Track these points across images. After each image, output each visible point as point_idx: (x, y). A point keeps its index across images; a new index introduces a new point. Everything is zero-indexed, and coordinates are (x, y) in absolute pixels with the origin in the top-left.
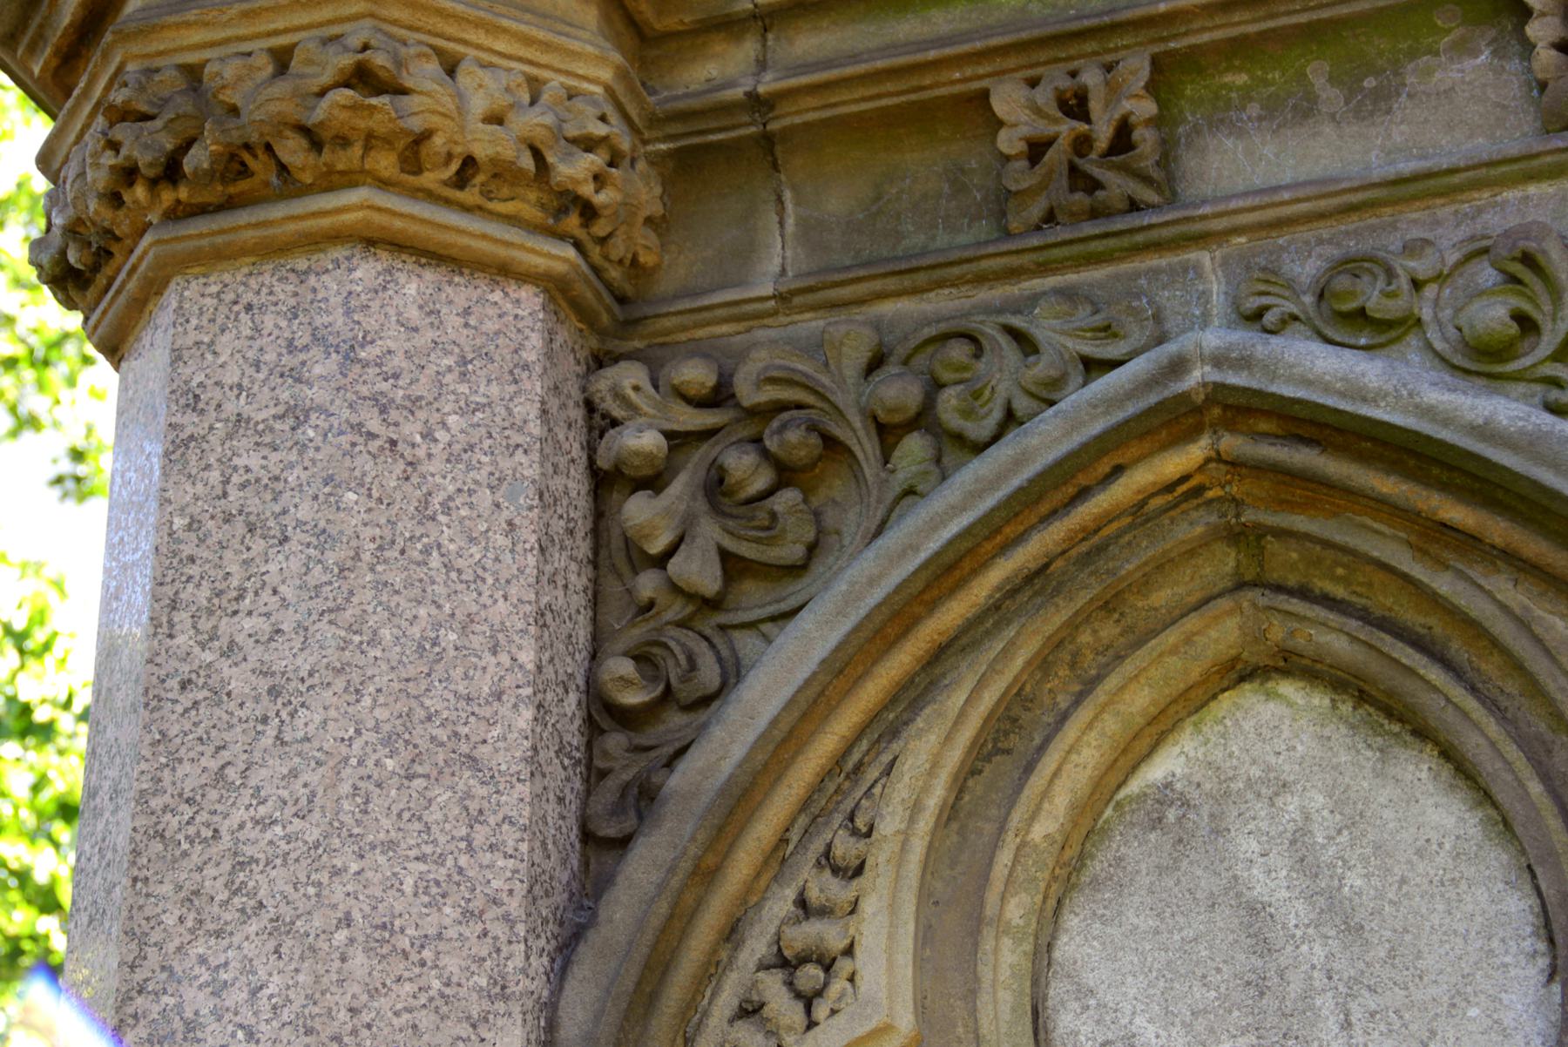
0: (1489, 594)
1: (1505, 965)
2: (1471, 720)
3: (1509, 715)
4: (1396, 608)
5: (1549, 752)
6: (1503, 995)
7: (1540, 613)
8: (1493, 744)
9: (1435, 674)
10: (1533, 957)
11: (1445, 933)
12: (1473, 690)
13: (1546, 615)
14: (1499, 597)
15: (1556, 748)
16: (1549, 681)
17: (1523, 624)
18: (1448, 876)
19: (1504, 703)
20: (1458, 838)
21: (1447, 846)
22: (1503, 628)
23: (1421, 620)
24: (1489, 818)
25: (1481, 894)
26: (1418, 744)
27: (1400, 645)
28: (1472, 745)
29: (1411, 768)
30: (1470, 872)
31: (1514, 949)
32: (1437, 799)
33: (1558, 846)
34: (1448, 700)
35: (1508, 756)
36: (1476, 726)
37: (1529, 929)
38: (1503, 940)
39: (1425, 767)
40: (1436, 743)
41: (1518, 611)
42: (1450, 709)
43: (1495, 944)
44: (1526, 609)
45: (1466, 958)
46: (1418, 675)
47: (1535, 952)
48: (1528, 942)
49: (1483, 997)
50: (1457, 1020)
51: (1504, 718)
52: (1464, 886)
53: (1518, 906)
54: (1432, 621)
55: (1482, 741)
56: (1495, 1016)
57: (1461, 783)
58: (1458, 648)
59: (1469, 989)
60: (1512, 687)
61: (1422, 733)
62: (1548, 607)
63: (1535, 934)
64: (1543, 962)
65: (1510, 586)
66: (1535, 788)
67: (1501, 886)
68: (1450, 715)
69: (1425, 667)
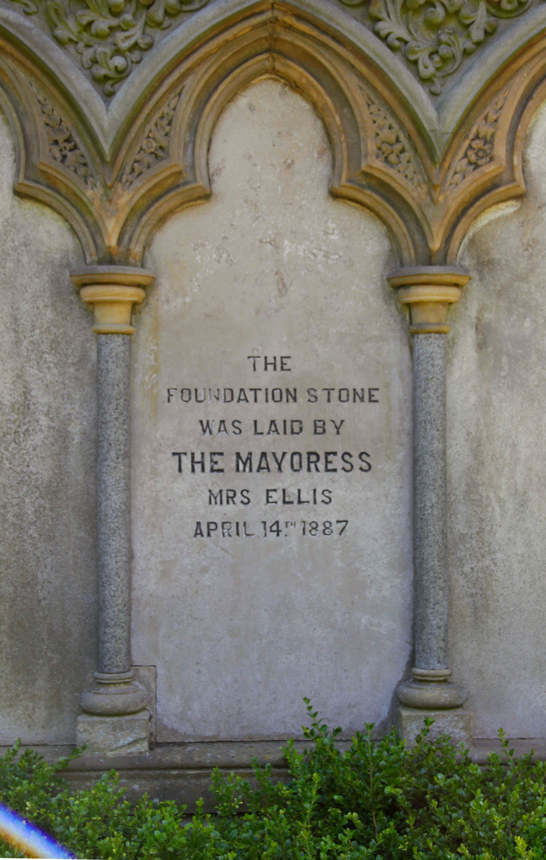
17: (14, 73)
22: (9, 72)
53: (9, 142)
64: (13, 157)
66: (14, 115)
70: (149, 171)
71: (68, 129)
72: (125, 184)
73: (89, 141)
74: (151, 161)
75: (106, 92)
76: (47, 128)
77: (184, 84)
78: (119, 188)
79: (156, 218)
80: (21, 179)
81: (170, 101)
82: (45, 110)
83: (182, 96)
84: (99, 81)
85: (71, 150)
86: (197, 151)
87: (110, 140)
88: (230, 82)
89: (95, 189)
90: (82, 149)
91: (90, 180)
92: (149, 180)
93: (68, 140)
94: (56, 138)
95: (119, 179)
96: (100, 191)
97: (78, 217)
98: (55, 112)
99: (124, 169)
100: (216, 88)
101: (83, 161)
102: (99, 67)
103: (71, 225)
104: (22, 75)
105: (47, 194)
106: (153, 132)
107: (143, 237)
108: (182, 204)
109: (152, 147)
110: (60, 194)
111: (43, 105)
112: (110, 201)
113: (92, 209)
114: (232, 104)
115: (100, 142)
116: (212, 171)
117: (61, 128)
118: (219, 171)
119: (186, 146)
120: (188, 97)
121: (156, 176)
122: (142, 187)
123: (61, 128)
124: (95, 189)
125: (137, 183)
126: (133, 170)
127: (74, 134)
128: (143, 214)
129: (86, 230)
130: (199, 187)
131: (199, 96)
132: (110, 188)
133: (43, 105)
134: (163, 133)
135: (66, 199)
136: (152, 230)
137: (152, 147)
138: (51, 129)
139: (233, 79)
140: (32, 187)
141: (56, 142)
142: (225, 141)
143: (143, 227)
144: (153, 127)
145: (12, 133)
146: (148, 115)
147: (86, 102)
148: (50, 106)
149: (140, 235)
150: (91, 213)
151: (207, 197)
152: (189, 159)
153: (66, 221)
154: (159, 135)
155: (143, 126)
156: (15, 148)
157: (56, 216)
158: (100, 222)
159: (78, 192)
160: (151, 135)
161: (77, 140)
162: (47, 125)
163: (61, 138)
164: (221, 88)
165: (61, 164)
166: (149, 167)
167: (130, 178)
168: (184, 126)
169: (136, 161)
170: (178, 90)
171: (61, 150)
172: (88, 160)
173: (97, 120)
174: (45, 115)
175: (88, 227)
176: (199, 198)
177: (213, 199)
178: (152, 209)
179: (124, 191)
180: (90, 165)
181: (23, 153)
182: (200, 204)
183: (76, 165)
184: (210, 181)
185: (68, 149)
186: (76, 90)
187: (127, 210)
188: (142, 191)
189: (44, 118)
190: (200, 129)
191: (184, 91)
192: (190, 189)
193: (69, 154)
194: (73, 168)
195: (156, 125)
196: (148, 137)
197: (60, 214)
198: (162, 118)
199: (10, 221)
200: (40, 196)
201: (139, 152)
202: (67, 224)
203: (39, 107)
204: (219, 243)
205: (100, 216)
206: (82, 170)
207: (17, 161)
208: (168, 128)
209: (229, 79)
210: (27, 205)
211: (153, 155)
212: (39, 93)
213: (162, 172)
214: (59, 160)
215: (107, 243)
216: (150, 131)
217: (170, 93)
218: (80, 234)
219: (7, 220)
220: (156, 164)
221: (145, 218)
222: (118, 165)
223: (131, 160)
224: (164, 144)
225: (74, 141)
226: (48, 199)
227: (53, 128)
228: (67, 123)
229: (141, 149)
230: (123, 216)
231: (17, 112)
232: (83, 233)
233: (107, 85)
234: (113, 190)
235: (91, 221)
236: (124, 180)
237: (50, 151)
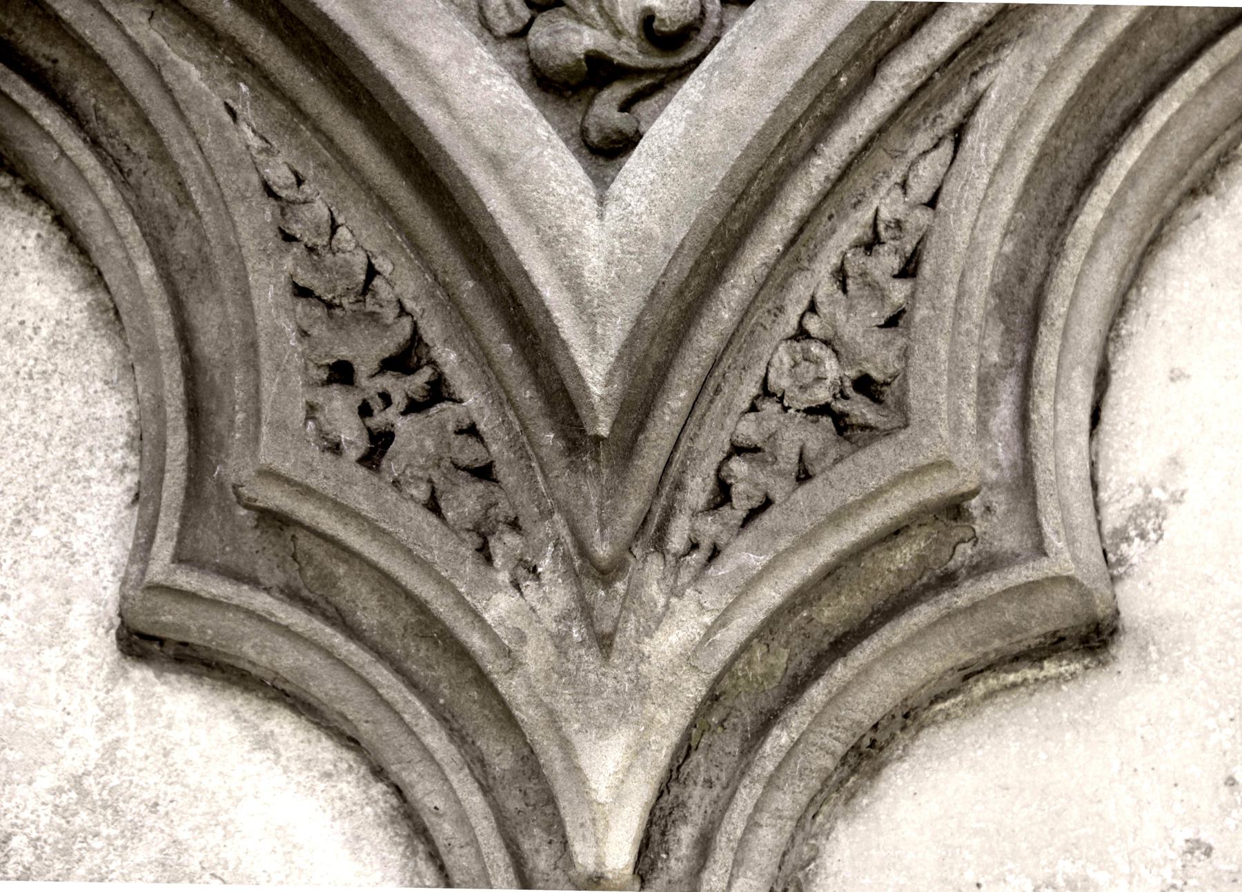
0: (118, 25)
1: (88, 480)
2: (86, 180)
3: (132, 180)
4: (18, 31)
5: (172, 229)
6: (78, 515)
7: (174, 56)
8: (106, 212)
9: (50, 118)
10: (122, 472)
11: (23, 436)
12: (94, 144)
13: (180, 60)
14: (129, 31)
15: (180, 225)
16: (174, 141)
17: (154, 69)
18: (39, 368)
19: (129, 164)
20: (58, 323)
21: (44, 332)
22: (130, 70)
23: (46, 50)
24: (99, 303)
25: (75, 394)
26: (29, 204)
27: (14, 76)
28: (84, 210)
29: (16, 233)
30: (65, 364)
31: (101, 461)
32: (41, 273)
33: (160, 342)
34: (63, 153)
35: (121, 229)
36: (91, 188)
37: (122, 439)
38: (90, 450)
39: (33, 233)
40: (52, 207)
41: (148, 51)
42: (64, 163)
43: (81, 453)
44: (159, 49)
45: (42, 467)
46: (30, 116)
47: (125, 466)
48: (120, 453)
49: (54, 515)
50: (19, 540)
51: (126, 182)
52: (55, 381)
53: (114, 411)
54: (58, 53)
55: (95, 206)
56: (65, 539)
57: (73, 258)
58: (84, 91)
59: (40, 505)
60: (140, 145)
61: (35, 192)
62: (184, 50)
63: (129, 446)
64: (131, 479)
65: (144, 19)
66: (146, 269)
67: (99, 385)
68: (63, 172)
69: (39, 108)
70: (801, 494)
71: (403, 312)
72: (680, 557)
73: (505, 350)
74: (813, 447)
75: (594, 136)
76: (301, 306)
77: (981, 84)
78: (652, 575)
79: (835, 741)
80: (160, 566)
81: (913, 164)
82: (296, 229)
83: (970, 139)
84: (561, 86)
85: (414, 407)
86: (1043, 407)
87: (615, 333)
88: (1203, 89)
89: (529, 586)
90: (472, 400)
91: (505, 545)
92: (808, 539)
93: (404, 360)
94: (344, 353)
95: (652, 532)
96: (553, 595)
97: (436, 740)
98: (343, 232)
99: (679, 486)
100: (1134, 117)
101: (470, 453)
102: (565, 23)
103: (398, 791)
104: (192, 72)
105: (286, 631)
106: (824, 309)
107: (769, 838)
108: (969, 674)
109: (819, 379)
110: (353, 632)
111: (284, 205)
112: (604, 643)
113: (511, 687)
114: (1207, 205)
115: (564, 345)
116: (1113, 517)
117: (370, 306)
118: (1148, 519)
119: (987, 386)
120: (999, 144)
121: (837, 518)
122: (765, 574)
123: (370, 306)
124: (529, 586)
125: (745, 556)
126: (723, 493)
127: (432, 331)
128: (767, 721)
129: (475, 802)
130: (1055, 580)
131: (1045, 156)
132: (606, 575)
133: (284, 205)
134: (877, 315)
135: (382, 654)
136: (814, 805)
137: (819, 379)
138: (319, 312)
139: (1217, 76)
140: (214, 602)
141: (342, 373)
142: (1176, 376)
143: (771, 783)
144: (826, 289)
145: (133, 363)
146: (804, 224)
147: (496, 163)
148: (320, 210)
149: (752, 824)
150: (507, 719)
151: (1094, 638)
152: (1004, 452)
153: (379, 772)
154: (856, 323)
155: (774, 281)
156: (145, 440)
157: (326, 751)
158: (550, 754)
159: (441, 605)
160: (813, 325)
161: (449, 358)
162: (302, 292)
163: (365, 350)
164: (1158, 116)
165: (362, 471)
166: (804, 476)
167: (710, 528)
168: (979, 302)
169: (737, 450)
170: (951, 114)
171: (365, 411)
172: (497, 448)
173: (548, 243)
174: (296, 249)
175: (486, 790)
176: (1053, 646)
177: (1124, 650)
178: (817, 693)
179: (675, 592)
180: (507, 474)
181: (177, 442)
182: (1059, 679)
183: (436, 475)
184: (1112, 565)
185: (399, 400)
186: (449, 108)
187: (694, 689)
188: (771, 596)
189: (288, 264)
190: (1057, 305)
191: (981, 118)
192: (1008, 592)
193: (404, 426)
194: (420, 492)
195: (841, 276)
196: (802, 334)
197: (351, 741)
198: (870, 244)
199: (88, 782)
200: (253, 649)
201: (753, 408)
202: (378, 789)
203: (269, 211)
204: (1167, 873)
205: (553, 719)
206: (466, 500)
207: (144, 497)
208: (899, 292)
209: (1201, 71)
210: (184, 704)
211: (826, 421)
212: (268, 151)
213: (872, 491)
214: (353, 454)
215: (584, 857)
216: (812, 308)
217: (912, 130)
218: (444, 831)
219: (77, 782)
220: (839, 460)
221: (780, 738)
222: (649, 462)
223: (710, 445)
224: (879, 358)
225: (432, 363)
226: (287, 659)
227: (330, 305)
228: (402, 281)
229: (766, 391)
230: (668, 721)
231: (161, 259)
232: (463, 820)
233: (599, 99)
234: (620, 586)
235: (502, 759)
236: (677, 542)
237: (311, 409)
